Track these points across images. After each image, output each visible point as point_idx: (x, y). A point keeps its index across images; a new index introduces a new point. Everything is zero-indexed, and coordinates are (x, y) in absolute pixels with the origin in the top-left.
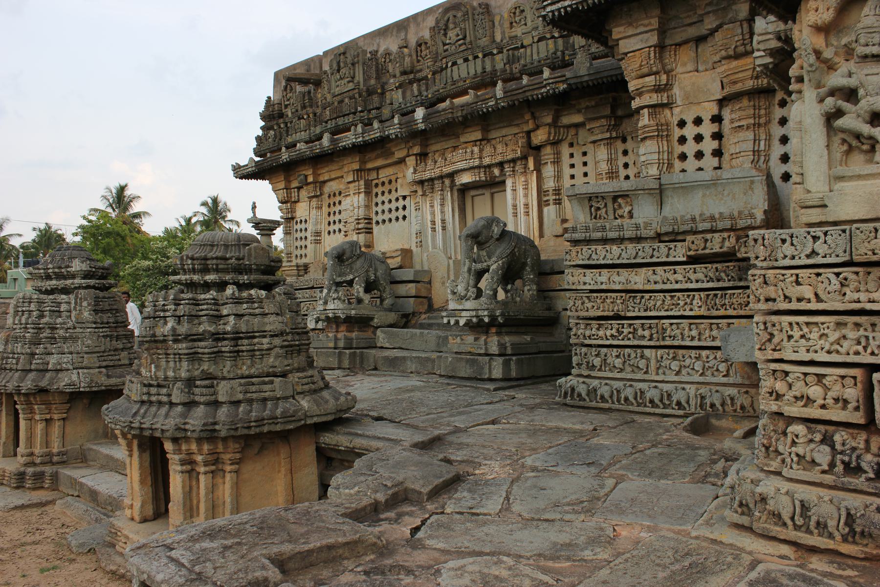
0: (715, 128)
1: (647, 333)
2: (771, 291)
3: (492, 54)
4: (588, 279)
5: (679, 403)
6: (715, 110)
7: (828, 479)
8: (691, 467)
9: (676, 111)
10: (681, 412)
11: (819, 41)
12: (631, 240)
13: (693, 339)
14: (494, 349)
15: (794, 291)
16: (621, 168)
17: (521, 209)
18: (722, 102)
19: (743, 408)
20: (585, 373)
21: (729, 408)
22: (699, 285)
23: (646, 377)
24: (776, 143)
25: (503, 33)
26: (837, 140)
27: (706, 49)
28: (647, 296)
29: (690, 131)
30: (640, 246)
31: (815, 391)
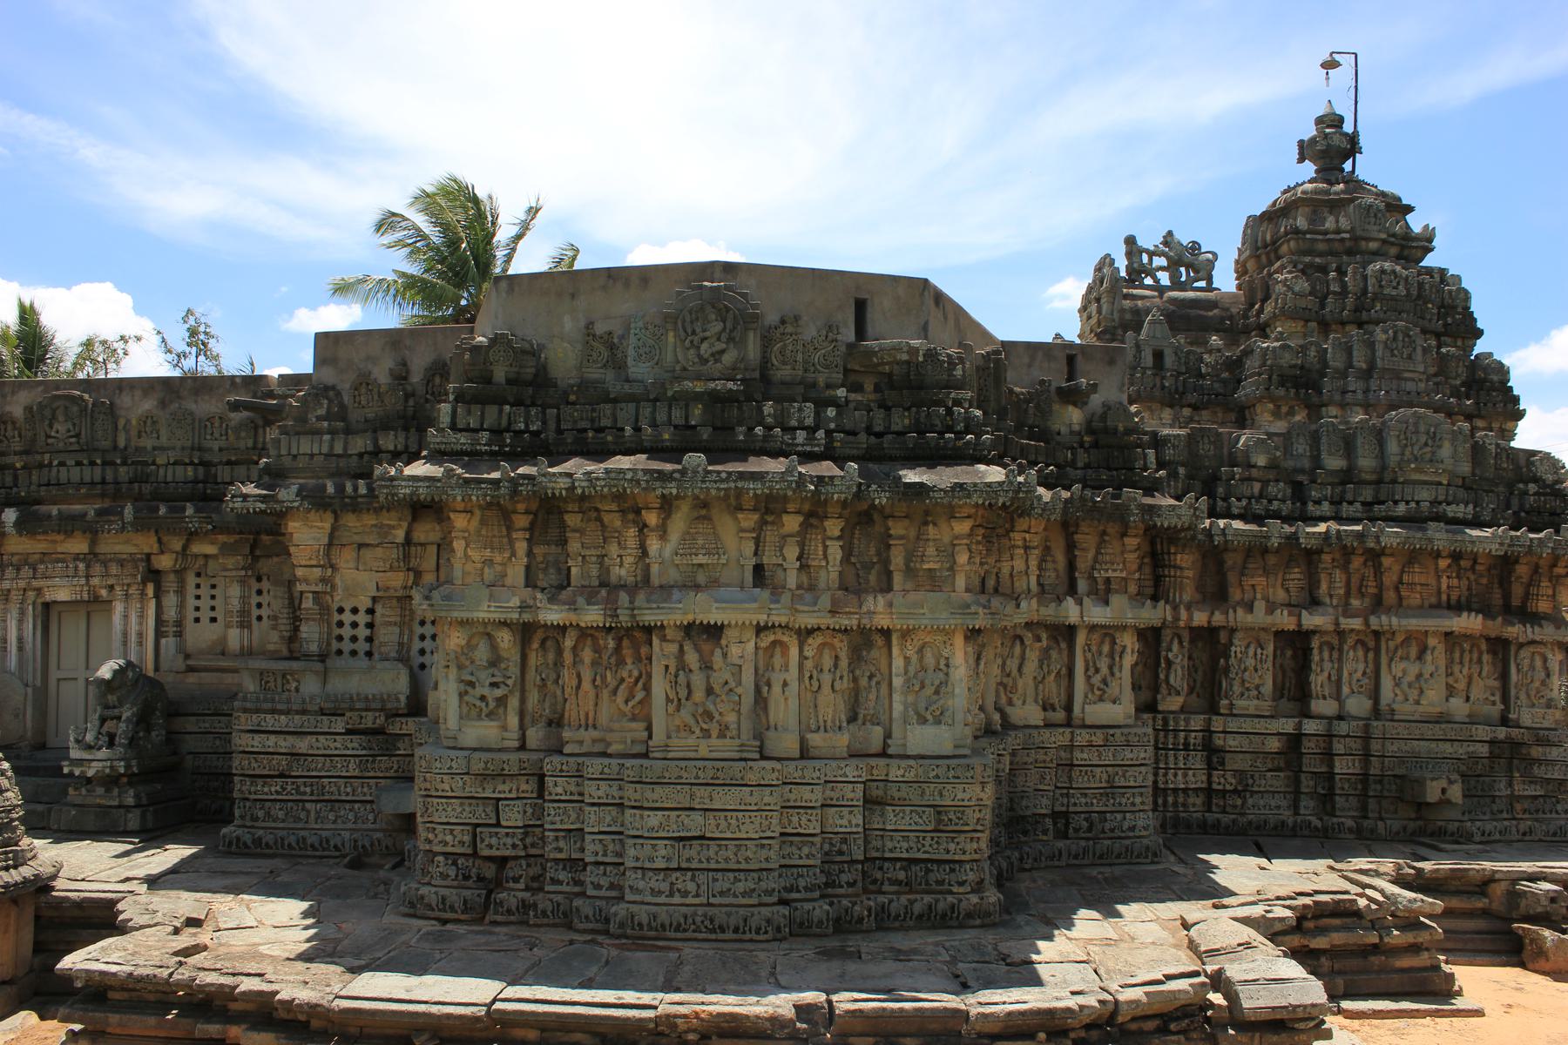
0: (368, 618)
1: (308, 790)
3: (113, 464)
5: (336, 847)
6: (370, 605)
7: (455, 883)
10: (337, 854)
12: (297, 712)
14: (130, 800)
15: (440, 786)
16: (254, 608)
17: (133, 638)
18: (374, 599)
19: (387, 847)
20: (249, 824)
23: (307, 826)
25: (128, 440)
27: (367, 554)
28: (310, 759)
29: (347, 617)
30: (305, 718)
31: (449, 838)
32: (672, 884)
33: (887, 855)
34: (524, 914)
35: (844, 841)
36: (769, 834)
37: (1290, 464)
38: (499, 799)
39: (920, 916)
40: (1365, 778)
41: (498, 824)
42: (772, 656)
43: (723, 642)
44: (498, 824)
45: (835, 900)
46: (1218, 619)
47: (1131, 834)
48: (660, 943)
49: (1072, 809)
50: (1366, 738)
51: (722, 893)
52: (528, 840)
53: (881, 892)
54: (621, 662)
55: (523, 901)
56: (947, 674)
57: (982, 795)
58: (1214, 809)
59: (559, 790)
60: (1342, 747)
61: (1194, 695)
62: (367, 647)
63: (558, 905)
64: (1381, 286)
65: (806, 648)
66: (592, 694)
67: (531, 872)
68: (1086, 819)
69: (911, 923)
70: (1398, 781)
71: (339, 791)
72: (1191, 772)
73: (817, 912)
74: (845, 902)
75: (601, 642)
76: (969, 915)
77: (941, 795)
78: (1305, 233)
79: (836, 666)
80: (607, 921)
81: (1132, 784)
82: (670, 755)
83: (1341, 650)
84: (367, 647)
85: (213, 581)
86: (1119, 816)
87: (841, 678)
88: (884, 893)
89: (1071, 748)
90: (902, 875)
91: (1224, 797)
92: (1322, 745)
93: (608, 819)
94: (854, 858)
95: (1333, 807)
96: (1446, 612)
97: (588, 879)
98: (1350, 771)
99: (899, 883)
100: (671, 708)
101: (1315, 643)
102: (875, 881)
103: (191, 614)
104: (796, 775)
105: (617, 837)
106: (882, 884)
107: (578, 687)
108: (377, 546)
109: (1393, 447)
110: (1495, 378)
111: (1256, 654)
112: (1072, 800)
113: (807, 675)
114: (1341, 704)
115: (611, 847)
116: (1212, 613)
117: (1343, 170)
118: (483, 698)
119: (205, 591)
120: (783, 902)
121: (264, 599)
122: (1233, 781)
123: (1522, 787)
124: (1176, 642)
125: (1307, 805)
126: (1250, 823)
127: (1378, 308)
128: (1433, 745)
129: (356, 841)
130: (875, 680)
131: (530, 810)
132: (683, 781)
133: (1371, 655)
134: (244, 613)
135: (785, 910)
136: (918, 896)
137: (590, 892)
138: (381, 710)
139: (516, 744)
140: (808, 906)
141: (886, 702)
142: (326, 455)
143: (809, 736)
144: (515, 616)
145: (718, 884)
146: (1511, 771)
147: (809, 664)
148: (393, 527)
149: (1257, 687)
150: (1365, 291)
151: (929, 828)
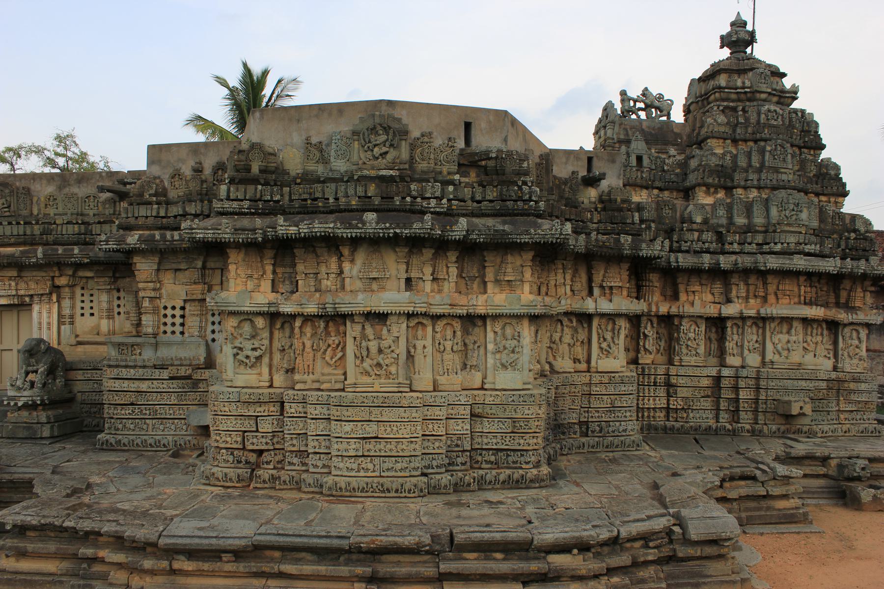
0: (181, 312)
1: (148, 412)
2: (216, 408)
3: (30, 223)
4: (116, 385)
5: (164, 445)
6: (182, 304)
7: (233, 465)
8: (180, 470)
9: (163, 301)
10: (165, 449)
11: (233, 330)
12: (140, 367)
13: (171, 414)
14: (44, 419)
17: (45, 326)
18: (185, 301)
19: (194, 445)
20: (113, 432)
21: (188, 446)
22: (174, 390)
23: (147, 433)
24: (210, 324)
25: (39, 210)
26: (236, 361)
27: (180, 275)
28: (148, 394)
29: (169, 312)
30: (145, 370)
31: (229, 439)
32: (359, 464)
33: (484, 447)
34: (273, 483)
35: (458, 439)
36: (415, 435)
37: (714, 221)
38: (258, 416)
39: (504, 482)
40: (756, 400)
41: (257, 431)
42: (417, 331)
43: (388, 323)
44: (257, 431)
45: (454, 473)
46: (674, 310)
47: (624, 434)
48: (353, 499)
49: (590, 420)
50: (758, 379)
51: (388, 470)
52: (275, 440)
53: (480, 468)
54: (328, 334)
55: (272, 475)
56: (519, 341)
57: (540, 412)
58: (671, 419)
59: (293, 410)
60: (743, 383)
61: (660, 354)
62: (181, 329)
63: (293, 477)
64: (768, 119)
65: (437, 327)
66: (311, 355)
67: (277, 458)
68: (598, 426)
69: (498, 486)
70: (775, 402)
71: (166, 413)
72: (657, 398)
73: (444, 480)
74: (460, 474)
76: (532, 481)
77: (515, 410)
78: (725, 88)
79: (454, 336)
80: (321, 486)
81: (625, 405)
82: (358, 390)
83: (743, 328)
84: (181, 329)
85: (92, 292)
86: (618, 424)
87: (457, 344)
88: (483, 469)
89: (590, 384)
90: (493, 458)
91: (676, 412)
92: (732, 383)
93: (322, 427)
94: (465, 449)
95: (739, 418)
96: (804, 306)
97: (310, 462)
98: (749, 397)
99: (492, 463)
100: (358, 362)
101: (729, 324)
102: (477, 462)
103: (79, 311)
104: (431, 401)
105: (326, 438)
106: (481, 463)
107: (303, 350)
108: (186, 270)
109: (774, 212)
110: (832, 173)
111: (695, 331)
112: (590, 415)
113: (437, 342)
114: (743, 359)
115: (323, 444)
116: (670, 307)
117: (746, 53)
118: (247, 357)
119: (87, 298)
120: (424, 474)
121: (121, 302)
122: (682, 403)
123: (844, 405)
124: (649, 324)
125: (724, 417)
126: (691, 427)
127: (766, 132)
128: (795, 382)
129: (176, 442)
130: (477, 345)
131: (276, 423)
132: (365, 405)
133: (760, 331)
134: (110, 310)
135: (425, 479)
136: (502, 470)
137: (311, 470)
138: (190, 365)
139: (267, 384)
140: (438, 477)
141: (483, 358)
142: (155, 217)
143: (438, 378)
144: (266, 309)
145: (386, 464)
146: (838, 396)
147: (438, 336)
148: (196, 259)
149: (696, 349)
150: (758, 122)
151: (508, 431)
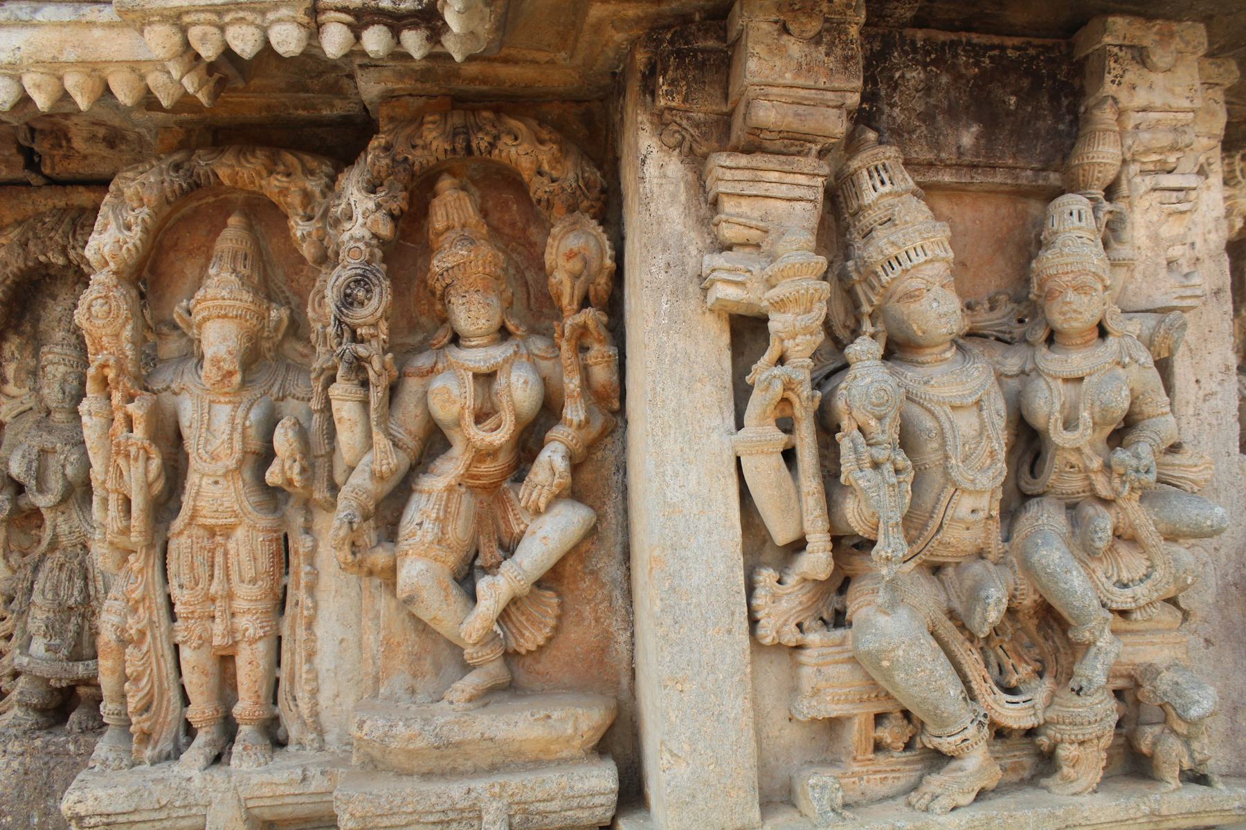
75: (299, 228)
